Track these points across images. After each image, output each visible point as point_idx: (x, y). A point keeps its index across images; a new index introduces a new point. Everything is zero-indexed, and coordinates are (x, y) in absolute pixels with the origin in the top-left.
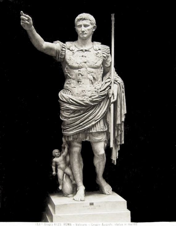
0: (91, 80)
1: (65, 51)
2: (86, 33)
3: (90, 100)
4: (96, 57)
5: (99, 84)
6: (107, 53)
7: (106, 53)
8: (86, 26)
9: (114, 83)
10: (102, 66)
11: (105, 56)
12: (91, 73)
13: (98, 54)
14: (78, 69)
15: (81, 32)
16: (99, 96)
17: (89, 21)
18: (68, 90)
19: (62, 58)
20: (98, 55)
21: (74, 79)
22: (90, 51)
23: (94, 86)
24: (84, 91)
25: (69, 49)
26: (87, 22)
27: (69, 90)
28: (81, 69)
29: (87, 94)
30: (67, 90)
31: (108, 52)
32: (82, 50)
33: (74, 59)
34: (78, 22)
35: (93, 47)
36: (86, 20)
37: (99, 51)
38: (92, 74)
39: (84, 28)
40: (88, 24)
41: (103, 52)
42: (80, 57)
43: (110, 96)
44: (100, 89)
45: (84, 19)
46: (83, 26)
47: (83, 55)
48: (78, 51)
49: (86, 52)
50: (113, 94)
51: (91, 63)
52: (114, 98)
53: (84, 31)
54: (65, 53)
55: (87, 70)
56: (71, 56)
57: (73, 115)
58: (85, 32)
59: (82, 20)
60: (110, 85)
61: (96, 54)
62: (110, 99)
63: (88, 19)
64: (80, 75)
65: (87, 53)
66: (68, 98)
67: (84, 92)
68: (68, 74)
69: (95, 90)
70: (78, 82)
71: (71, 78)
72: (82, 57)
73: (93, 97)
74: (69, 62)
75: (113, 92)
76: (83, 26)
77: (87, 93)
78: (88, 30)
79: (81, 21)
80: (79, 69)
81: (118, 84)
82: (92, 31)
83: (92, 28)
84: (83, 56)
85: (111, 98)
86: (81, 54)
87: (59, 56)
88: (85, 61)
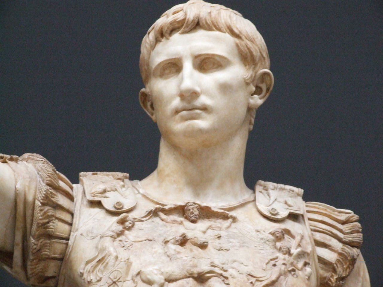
1: (72, 215)
2: (205, 109)
4: (269, 252)
6: (340, 240)
7: (334, 243)
11: (330, 256)
13: (286, 236)
15: (176, 102)
17: (228, 36)
19: (46, 252)
20: (292, 244)
22: (234, 219)
25: (98, 204)
26: (218, 40)
31: (349, 238)
32: (182, 210)
33: (123, 255)
34: (159, 47)
35: (254, 200)
39: (197, 74)
41: (319, 236)
42: (166, 242)
46: (188, 66)
47: (189, 235)
48: (154, 213)
49: (202, 225)
53: (195, 95)
54: (71, 224)
56: (107, 243)
58: (204, 100)
59: (184, 33)
61: (273, 234)
65: (210, 227)
72: (179, 248)
74: (92, 277)
76: (188, 66)
79: (176, 36)
82: (249, 109)
84: (183, 241)
87: (25, 239)
88: (204, 267)
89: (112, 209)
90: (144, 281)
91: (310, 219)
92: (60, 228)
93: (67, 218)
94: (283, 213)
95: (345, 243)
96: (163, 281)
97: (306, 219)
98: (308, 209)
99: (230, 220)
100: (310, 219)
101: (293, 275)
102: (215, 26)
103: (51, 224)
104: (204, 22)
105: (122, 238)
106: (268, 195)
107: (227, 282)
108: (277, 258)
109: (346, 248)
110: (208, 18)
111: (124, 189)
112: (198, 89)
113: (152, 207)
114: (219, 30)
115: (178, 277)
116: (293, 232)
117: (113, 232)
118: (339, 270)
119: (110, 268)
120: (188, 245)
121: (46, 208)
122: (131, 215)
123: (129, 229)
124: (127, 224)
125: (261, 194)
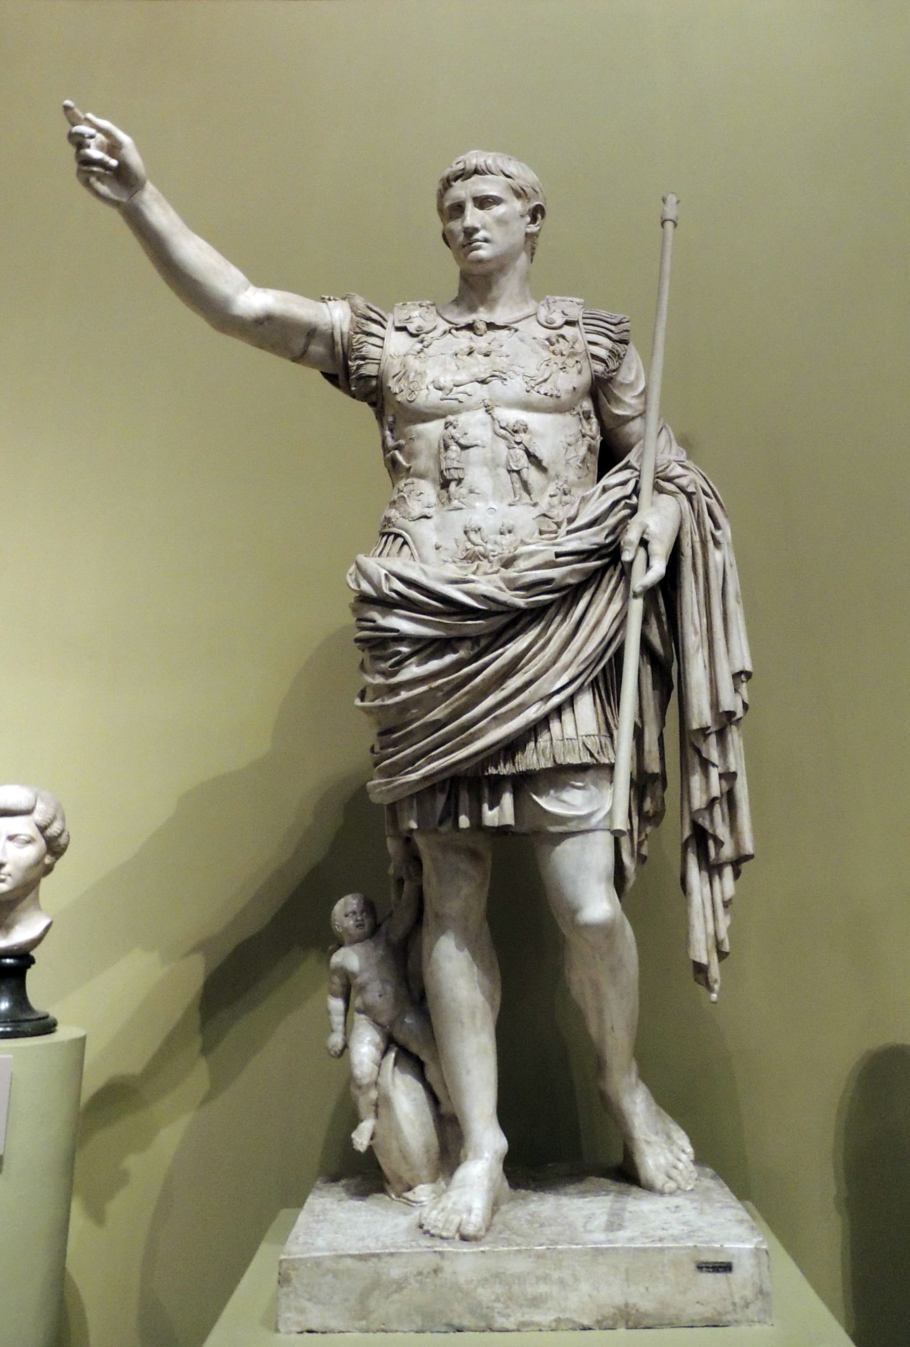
0: (518, 472)
1: (383, 339)
2: (486, 240)
3: (504, 580)
5: (565, 498)
8: (483, 202)
9: (659, 490)
10: (587, 405)
12: (516, 432)
13: (560, 339)
14: (444, 416)
16: (558, 555)
17: (503, 178)
18: (392, 537)
19: (363, 371)
21: (421, 476)
22: (516, 330)
23: (535, 505)
24: (478, 530)
27: (397, 536)
28: (462, 419)
29: (489, 547)
30: (389, 534)
36: (486, 174)
37: (567, 331)
38: (522, 435)
40: (493, 192)
43: (626, 557)
44: (571, 520)
45: (476, 172)
50: (644, 543)
51: (515, 387)
52: (651, 563)
53: (476, 230)
55: (493, 419)
57: (413, 671)
60: (629, 497)
62: (626, 572)
63: (493, 170)
64: (454, 447)
66: (384, 572)
67: (473, 536)
68: (400, 457)
69: (544, 528)
70: (445, 484)
71: (409, 469)
72: (468, 358)
73: (522, 564)
75: (643, 533)
76: (470, 206)
77: (496, 543)
78: (501, 221)
80: (450, 418)
81: (683, 497)
83: (522, 216)
85: (631, 563)
86: (465, 339)
89: (414, 332)
90: (436, 388)
91: (585, 324)
92: (374, 352)
93: (378, 342)
94: (559, 320)
95: (614, 341)
96: (452, 386)
97: (581, 324)
98: (586, 316)
99: (513, 331)
100: (585, 324)
101: (564, 372)
102: (489, 172)
103: (364, 348)
104: (480, 169)
105: (422, 355)
106: (549, 309)
107: (505, 383)
108: (550, 359)
109: (616, 346)
110: (483, 164)
111: (427, 314)
112: (478, 225)
113: (448, 326)
114: (492, 174)
115: (464, 382)
116: (567, 336)
117: (414, 350)
118: (610, 364)
119: (411, 380)
120: (475, 354)
121: (359, 336)
122: (430, 335)
123: (427, 347)
124: (425, 343)
125: (542, 307)
